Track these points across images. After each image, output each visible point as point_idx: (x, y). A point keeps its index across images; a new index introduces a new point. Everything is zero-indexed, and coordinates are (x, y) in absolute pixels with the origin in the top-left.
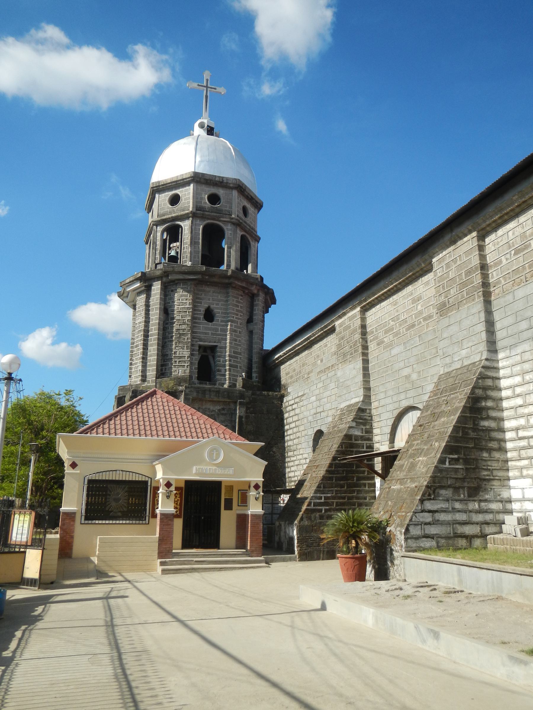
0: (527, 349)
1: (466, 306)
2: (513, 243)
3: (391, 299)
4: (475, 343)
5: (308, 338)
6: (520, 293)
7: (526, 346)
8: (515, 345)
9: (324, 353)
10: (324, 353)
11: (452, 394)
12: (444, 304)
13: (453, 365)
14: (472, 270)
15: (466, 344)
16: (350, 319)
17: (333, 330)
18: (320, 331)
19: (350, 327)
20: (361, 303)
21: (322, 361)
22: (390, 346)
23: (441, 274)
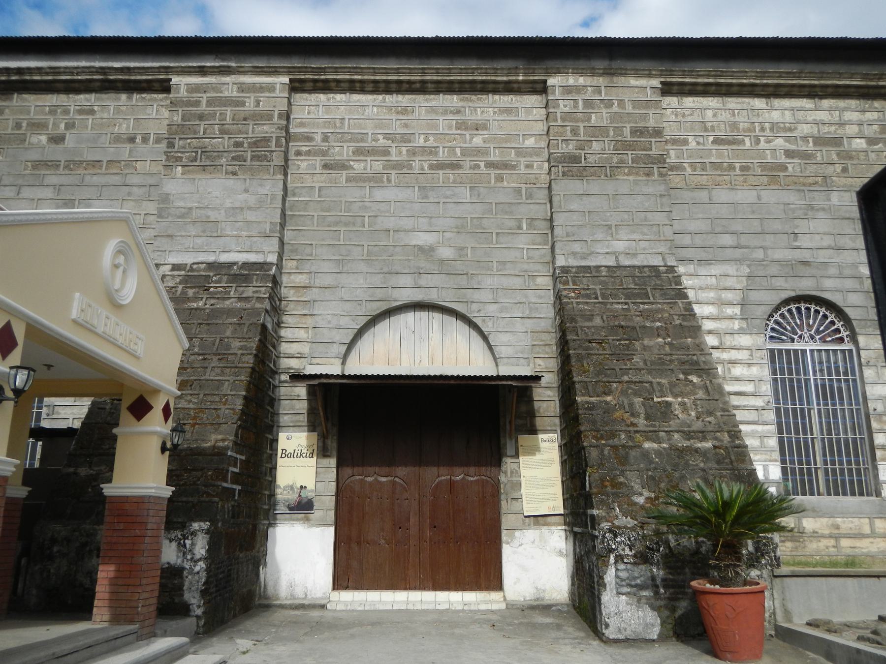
0: (731, 273)
1: (631, 178)
2: (712, 126)
3: (380, 97)
4: (648, 237)
5: (19, 71)
6: (722, 196)
7: (730, 269)
8: (708, 262)
9: (70, 126)
10: (70, 126)
11: (641, 303)
12: (575, 159)
13: (592, 257)
14: (648, 131)
15: (623, 234)
16: (242, 88)
17: (165, 87)
18: (92, 73)
19: (243, 104)
20: (300, 70)
21: (58, 139)
22: (376, 180)
23: (567, 109)
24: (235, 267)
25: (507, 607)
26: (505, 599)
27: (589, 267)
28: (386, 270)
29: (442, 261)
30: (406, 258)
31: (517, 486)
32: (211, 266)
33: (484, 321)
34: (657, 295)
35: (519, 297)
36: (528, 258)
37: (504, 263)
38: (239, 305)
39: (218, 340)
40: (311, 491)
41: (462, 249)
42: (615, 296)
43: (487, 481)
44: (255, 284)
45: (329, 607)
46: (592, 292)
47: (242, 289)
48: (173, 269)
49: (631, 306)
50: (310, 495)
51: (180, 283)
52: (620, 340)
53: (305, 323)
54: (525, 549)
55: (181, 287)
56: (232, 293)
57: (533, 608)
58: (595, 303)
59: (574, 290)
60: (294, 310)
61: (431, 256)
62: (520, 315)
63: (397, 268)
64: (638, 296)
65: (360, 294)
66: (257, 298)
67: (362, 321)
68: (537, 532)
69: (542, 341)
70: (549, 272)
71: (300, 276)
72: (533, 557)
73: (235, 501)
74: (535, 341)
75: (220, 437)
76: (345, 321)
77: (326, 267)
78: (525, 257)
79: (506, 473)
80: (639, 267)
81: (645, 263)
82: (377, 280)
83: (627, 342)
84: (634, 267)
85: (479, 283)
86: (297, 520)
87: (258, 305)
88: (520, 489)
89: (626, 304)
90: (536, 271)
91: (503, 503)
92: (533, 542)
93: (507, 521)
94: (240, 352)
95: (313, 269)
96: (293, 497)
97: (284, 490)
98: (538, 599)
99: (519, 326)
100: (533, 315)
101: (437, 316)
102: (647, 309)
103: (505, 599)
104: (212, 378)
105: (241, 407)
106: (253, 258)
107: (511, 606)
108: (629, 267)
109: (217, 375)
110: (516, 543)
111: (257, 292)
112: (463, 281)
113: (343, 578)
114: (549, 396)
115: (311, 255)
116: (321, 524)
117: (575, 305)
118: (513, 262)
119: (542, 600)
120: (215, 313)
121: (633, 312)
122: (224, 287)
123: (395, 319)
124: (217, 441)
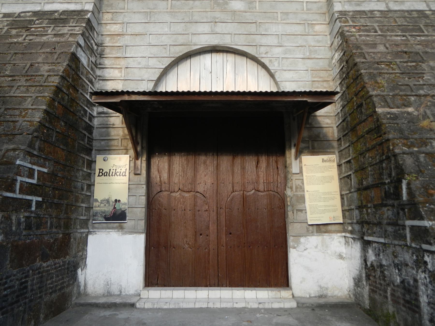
11: (418, 36)
24: (56, 14)
25: (298, 307)
26: (293, 296)
27: (364, 12)
28: (187, 20)
29: (234, 12)
30: (204, 10)
31: (302, 199)
32: (35, 13)
33: (270, 61)
34: (430, 30)
35: (300, 41)
36: (308, 10)
37: (287, 14)
38: (54, 39)
39: (28, 65)
40: (125, 204)
41: (251, 3)
42: (393, 31)
43: (275, 196)
44: (71, 24)
45: (138, 305)
46: (371, 28)
47: (59, 28)
48: (4, 17)
49: (409, 37)
50: (123, 207)
51: (7, 26)
52: (406, 62)
53: (119, 65)
54: (309, 253)
55: (6, 28)
56: (49, 31)
57: (322, 306)
58: (376, 36)
59: (354, 27)
60: (109, 53)
61: (225, 8)
62: (302, 56)
63: (196, 18)
64: (413, 30)
65: (165, 40)
66: (71, 34)
67: (167, 62)
68: (320, 238)
69: (320, 77)
70: (325, 21)
71: (115, 26)
72: (316, 260)
73: (32, 212)
74: (315, 77)
75: (12, 147)
76: (153, 62)
77: (137, 18)
78: (305, 9)
79: (291, 188)
80: (407, 11)
81: (412, 8)
82: (179, 28)
83: (414, 64)
84: (403, 11)
85: (266, 30)
86: (113, 228)
87: (71, 39)
88: (304, 202)
89: (404, 36)
90: (314, 20)
91: (290, 214)
92: (316, 247)
93: (293, 229)
94: (48, 73)
95: (126, 20)
96: (109, 209)
97: (101, 203)
98: (321, 297)
99: (301, 65)
100: (313, 56)
101: (231, 57)
102: (424, 40)
103: (293, 296)
104: (15, 95)
105: (38, 120)
106: (72, 7)
107: (302, 305)
108: (399, 11)
109: (22, 92)
110: (301, 247)
111: (72, 30)
112: (252, 28)
113: (157, 273)
114: (327, 124)
115: (124, 9)
116: (134, 231)
117: (358, 37)
118: (295, 13)
119: (326, 296)
120: (31, 45)
121: (412, 42)
122: (43, 28)
123: (195, 60)
124: (8, 150)
